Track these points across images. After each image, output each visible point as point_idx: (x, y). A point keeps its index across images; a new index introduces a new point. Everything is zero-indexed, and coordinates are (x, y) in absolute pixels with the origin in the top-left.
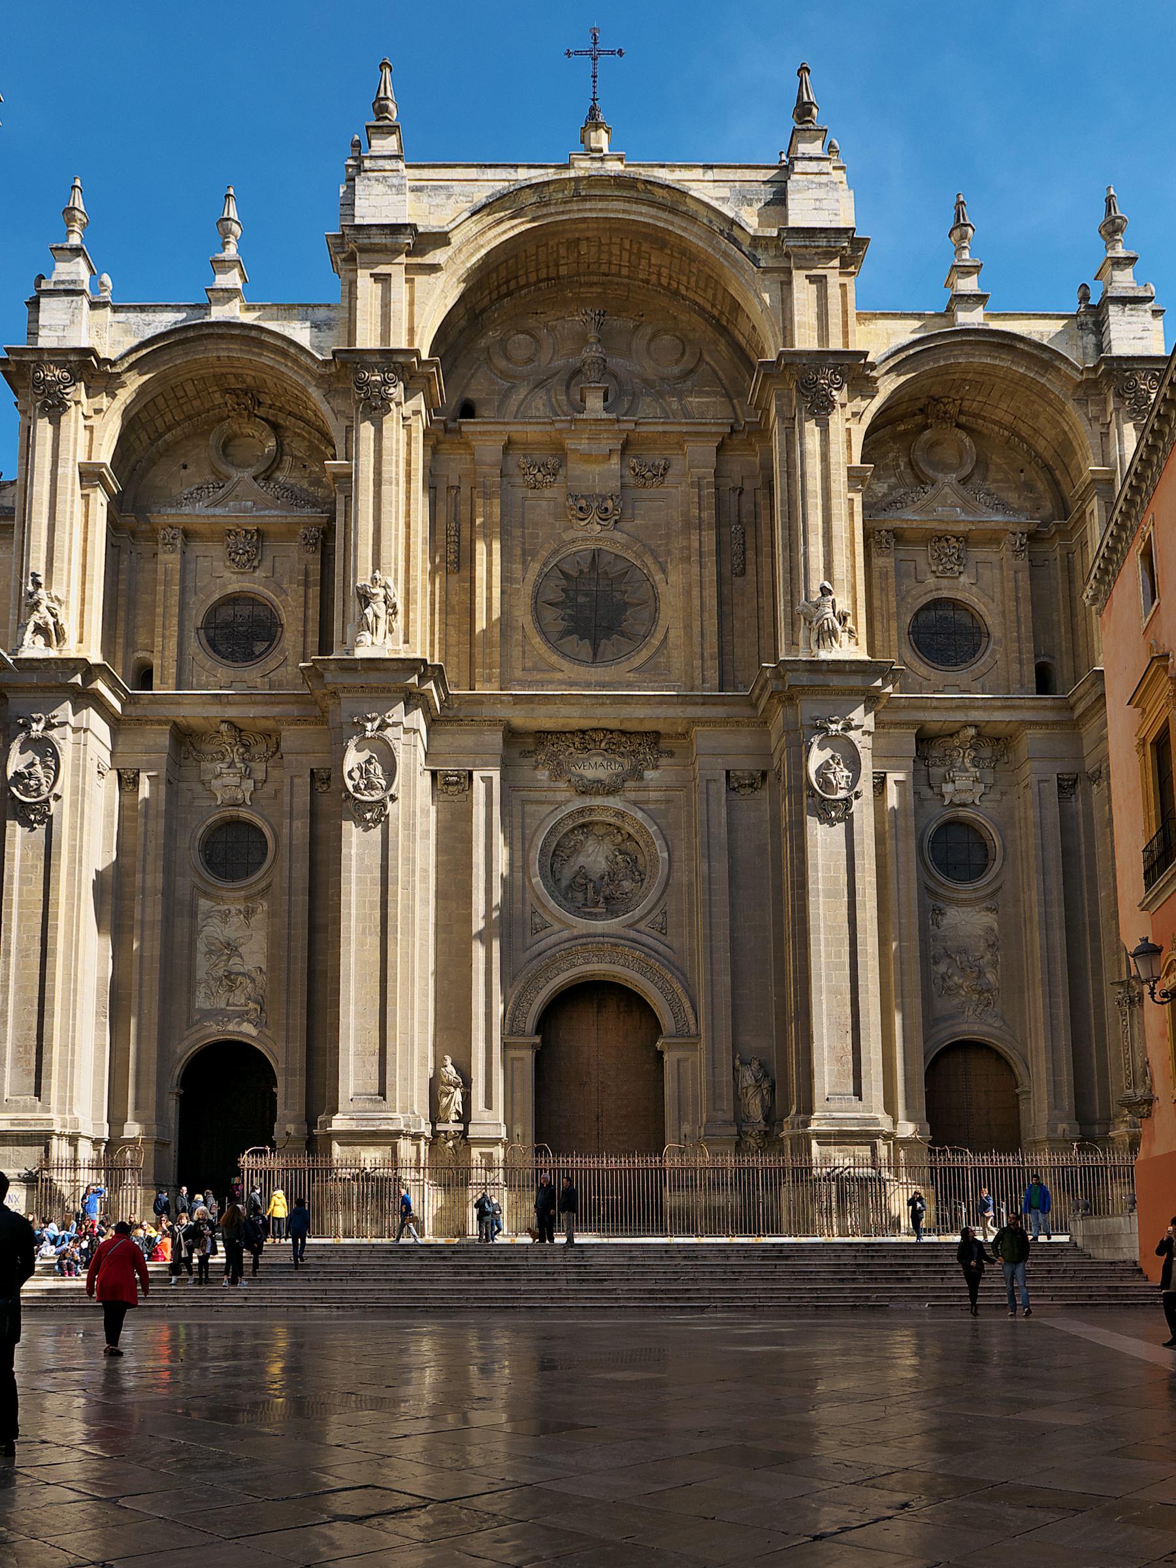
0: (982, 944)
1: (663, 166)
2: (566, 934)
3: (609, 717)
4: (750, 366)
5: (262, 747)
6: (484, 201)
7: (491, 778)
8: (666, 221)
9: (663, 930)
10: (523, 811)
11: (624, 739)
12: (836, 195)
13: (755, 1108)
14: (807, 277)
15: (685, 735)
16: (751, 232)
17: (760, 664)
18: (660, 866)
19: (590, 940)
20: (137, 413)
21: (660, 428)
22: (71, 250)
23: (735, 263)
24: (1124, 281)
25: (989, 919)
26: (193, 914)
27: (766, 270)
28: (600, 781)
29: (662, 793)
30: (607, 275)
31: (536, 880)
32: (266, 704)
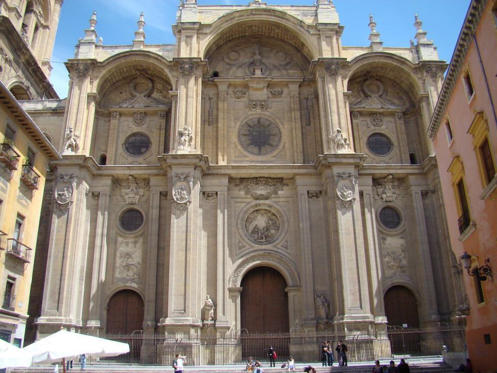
0: (400, 250)
1: (278, 6)
2: (251, 250)
3: (265, 173)
4: (309, 62)
6: (222, 15)
7: (224, 194)
9: (286, 248)
11: (270, 180)
13: (323, 312)
15: (292, 179)
16: (307, 24)
17: (317, 156)
21: (280, 80)
22: (91, 31)
23: (302, 32)
24: (424, 40)
25: (402, 241)
26: (116, 243)
27: (313, 35)
31: (241, 231)
32: (145, 169)
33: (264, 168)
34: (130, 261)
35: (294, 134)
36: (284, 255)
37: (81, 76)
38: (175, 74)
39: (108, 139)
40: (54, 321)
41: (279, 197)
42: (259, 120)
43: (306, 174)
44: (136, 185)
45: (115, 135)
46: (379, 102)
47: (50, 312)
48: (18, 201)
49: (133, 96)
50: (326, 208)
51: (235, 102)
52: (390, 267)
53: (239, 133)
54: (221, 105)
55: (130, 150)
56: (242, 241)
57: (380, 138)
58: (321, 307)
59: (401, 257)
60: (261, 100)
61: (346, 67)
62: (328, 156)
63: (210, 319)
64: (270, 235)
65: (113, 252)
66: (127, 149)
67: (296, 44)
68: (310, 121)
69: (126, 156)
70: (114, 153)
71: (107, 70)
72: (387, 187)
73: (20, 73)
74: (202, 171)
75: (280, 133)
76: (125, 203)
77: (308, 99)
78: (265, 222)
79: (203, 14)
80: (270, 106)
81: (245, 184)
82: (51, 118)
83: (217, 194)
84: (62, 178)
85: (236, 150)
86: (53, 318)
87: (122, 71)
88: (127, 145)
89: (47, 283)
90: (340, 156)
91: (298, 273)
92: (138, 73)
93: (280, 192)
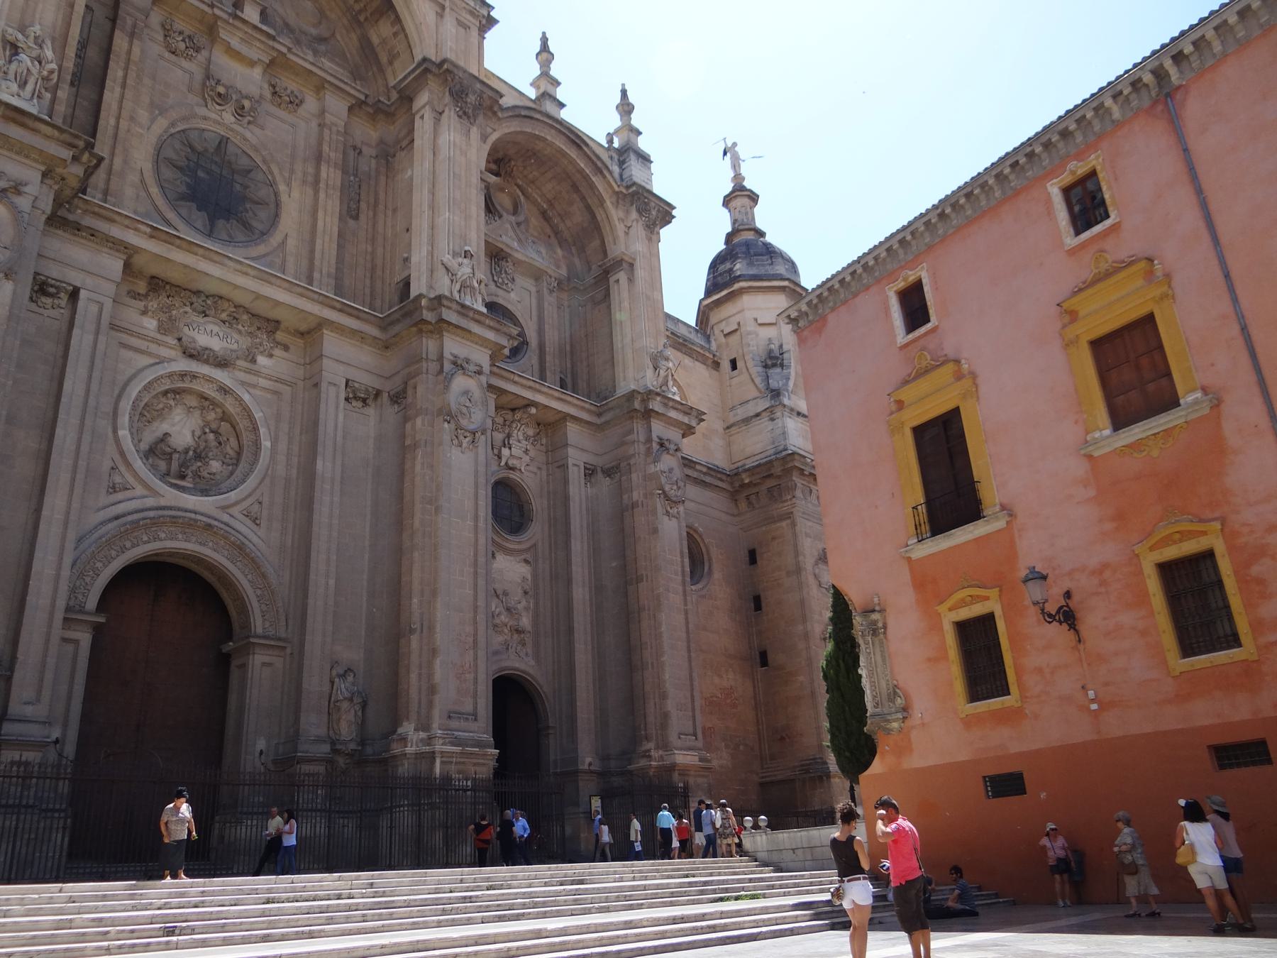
0: (520, 591)
2: (150, 502)
9: (254, 520)
11: (245, 317)
25: (525, 570)
28: (214, 351)
29: (270, 383)
31: (124, 433)
33: (246, 274)
35: (320, 223)
41: (257, 373)
42: (223, 142)
43: (354, 333)
51: (161, 57)
52: (495, 626)
53: (158, 151)
56: (123, 468)
59: (519, 606)
61: (490, 114)
64: (205, 474)
75: (278, 204)
78: (193, 432)
81: (163, 299)
85: (143, 194)
93: (262, 360)
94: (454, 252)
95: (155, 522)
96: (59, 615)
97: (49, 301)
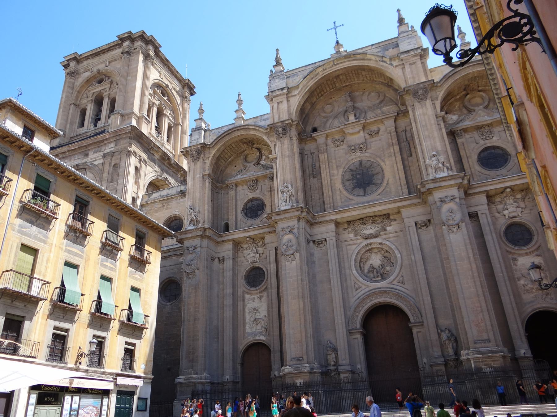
2: (367, 290)
5: (260, 243)
6: (307, 74)
8: (362, 63)
9: (403, 283)
10: (347, 249)
11: (377, 218)
12: (415, 39)
14: (409, 64)
18: (398, 259)
19: (376, 290)
20: (219, 155)
26: (244, 300)
28: (371, 234)
30: (350, 82)
34: (258, 316)
36: (401, 291)
37: (195, 160)
38: (272, 139)
39: (228, 209)
40: (190, 380)
41: (388, 234)
42: (361, 162)
43: (411, 205)
44: (255, 245)
45: (234, 204)
46: (485, 114)
47: (186, 372)
48: (130, 276)
49: (245, 167)
50: (436, 236)
53: (343, 180)
54: (322, 157)
55: (249, 215)
56: (357, 282)
57: (493, 151)
58: (447, 342)
60: (360, 143)
61: (435, 88)
62: (425, 183)
63: (333, 363)
64: (385, 272)
65: (242, 309)
66: (246, 214)
67: (385, 81)
68: (411, 151)
69: (245, 220)
70: (234, 220)
71: (216, 150)
72: (508, 202)
73: (157, 168)
74: (308, 222)
75: (383, 170)
76: (248, 263)
77: (406, 131)
79: (291, 79)
80: (369, 147)
81: (352, 226)
82: (181, 200)
83: (326, 239)
84: (188, 250)
86: (189, 376)
87: (231, 147)
88: (245, 211)
89: (183, 345)
90: (438, 180)
91: (418, 308)
92: (246, 146)
93: (388, 228)
94: (431, 157)
95: (369, 296)
96: (345, 333)
97: (321, 245)
